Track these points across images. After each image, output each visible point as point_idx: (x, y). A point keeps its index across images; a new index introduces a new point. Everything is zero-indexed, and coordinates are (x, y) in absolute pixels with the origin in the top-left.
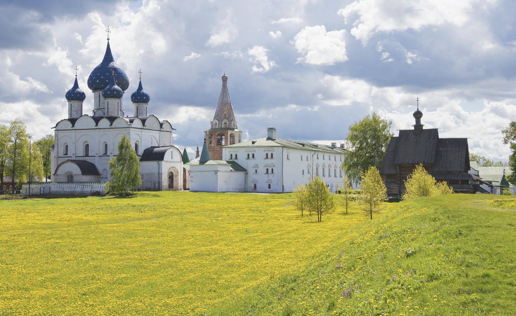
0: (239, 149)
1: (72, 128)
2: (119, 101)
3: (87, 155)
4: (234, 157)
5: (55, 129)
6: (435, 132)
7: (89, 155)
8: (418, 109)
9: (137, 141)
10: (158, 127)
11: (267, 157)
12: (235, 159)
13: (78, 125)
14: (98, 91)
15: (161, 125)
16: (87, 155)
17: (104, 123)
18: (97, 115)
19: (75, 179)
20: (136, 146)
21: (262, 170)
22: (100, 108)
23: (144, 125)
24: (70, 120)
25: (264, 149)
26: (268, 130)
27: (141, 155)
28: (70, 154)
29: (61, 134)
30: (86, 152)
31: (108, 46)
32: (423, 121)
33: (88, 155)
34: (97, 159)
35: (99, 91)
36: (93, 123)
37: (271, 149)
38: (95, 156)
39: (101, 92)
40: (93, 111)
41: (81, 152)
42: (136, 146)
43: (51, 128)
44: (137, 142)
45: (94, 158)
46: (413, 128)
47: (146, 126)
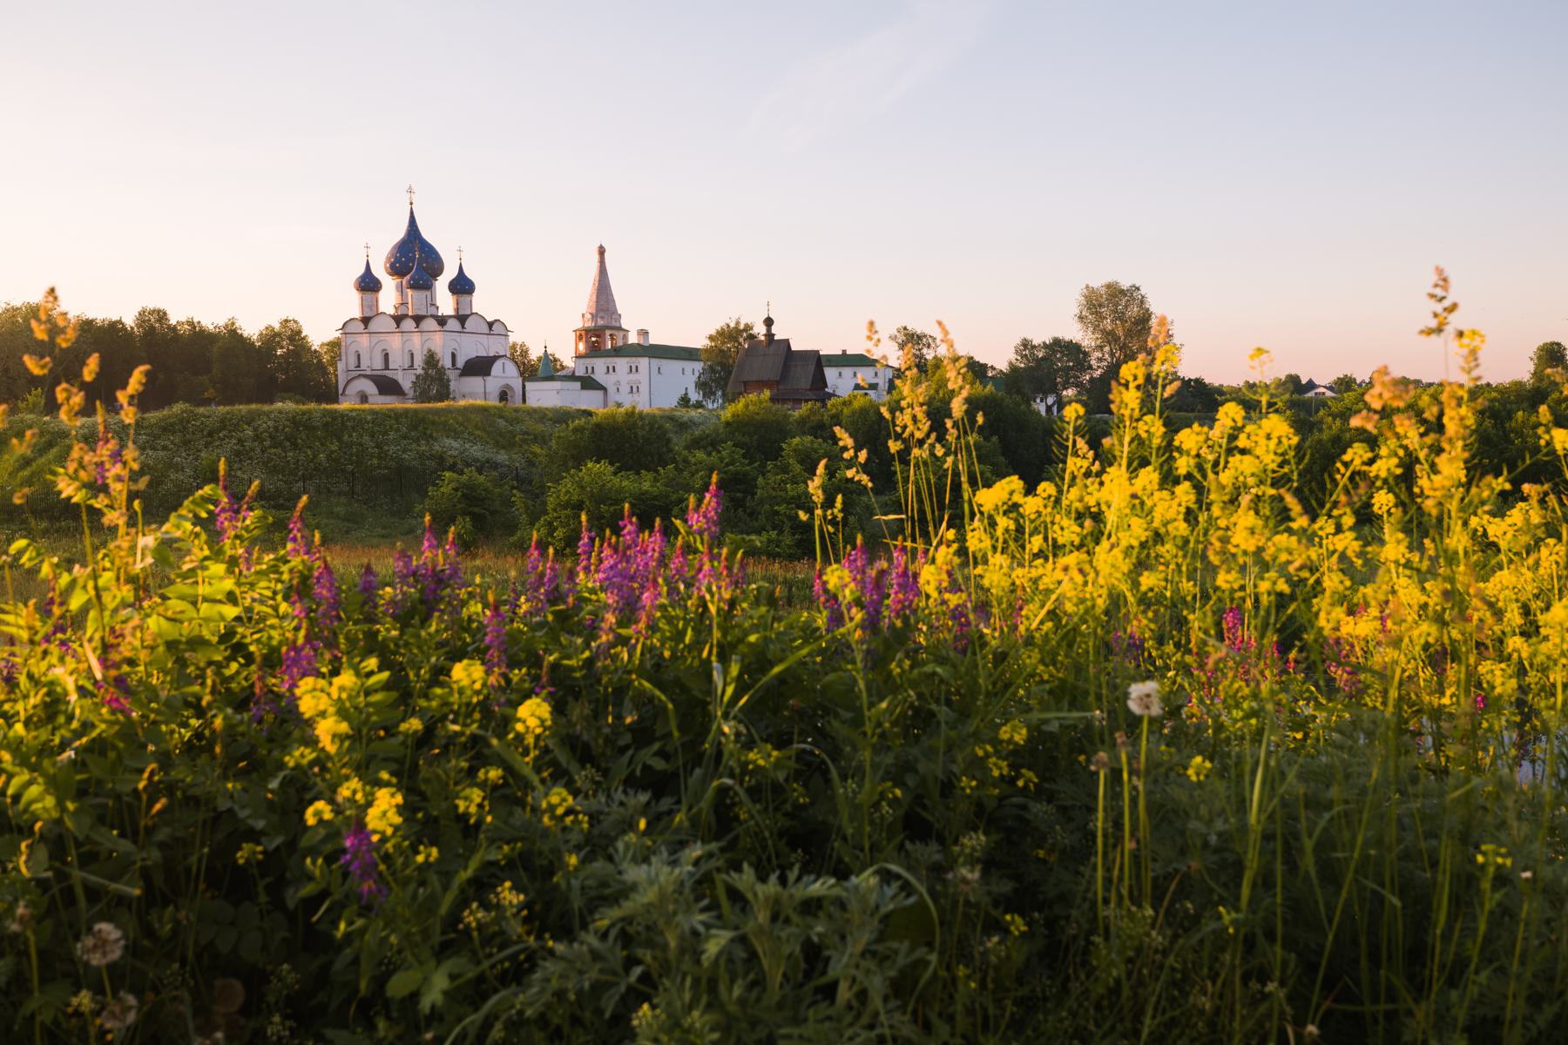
2: (428, 293)
6: (787, 342)
13: (373, 326)
16: (387, 368)
17: (409, 324)
19: (370, 399)
21: (625, 389)
28: (363, 366)
29: (350, 339)
31: (412, 213)
32: (774, 330)
34: (400, 373)
41: (378, 363)
42: (453, 355)
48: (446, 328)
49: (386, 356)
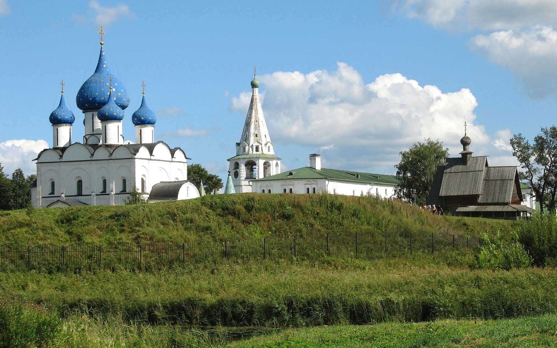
0: (272, 182)
1: (59, 160)
3: (80, 194)
5: (36, 161)
7: (83, 194)
8: (465, 135)
9: (144, 175)
13: (67, 156)
14: (90, 112)
15: (173, 152)
16: (80, 194)
18: (90, 142)
20: (143, 182)
24: (55, 149)
25: (304, 182)
26: (311, 158)
27: (149, 193)
29: (44, 167)
30: (78, 190)
32: (470, 149)
33: (82, 193)
36: (85, 154)
37: (312, 181)
38: (91, 195)
39: (96, 113)
40: (84, 137)
42: (143, 182)
44: (143, 177)
45: (89, 197)
46: (460, 156)
49: (80, 183)
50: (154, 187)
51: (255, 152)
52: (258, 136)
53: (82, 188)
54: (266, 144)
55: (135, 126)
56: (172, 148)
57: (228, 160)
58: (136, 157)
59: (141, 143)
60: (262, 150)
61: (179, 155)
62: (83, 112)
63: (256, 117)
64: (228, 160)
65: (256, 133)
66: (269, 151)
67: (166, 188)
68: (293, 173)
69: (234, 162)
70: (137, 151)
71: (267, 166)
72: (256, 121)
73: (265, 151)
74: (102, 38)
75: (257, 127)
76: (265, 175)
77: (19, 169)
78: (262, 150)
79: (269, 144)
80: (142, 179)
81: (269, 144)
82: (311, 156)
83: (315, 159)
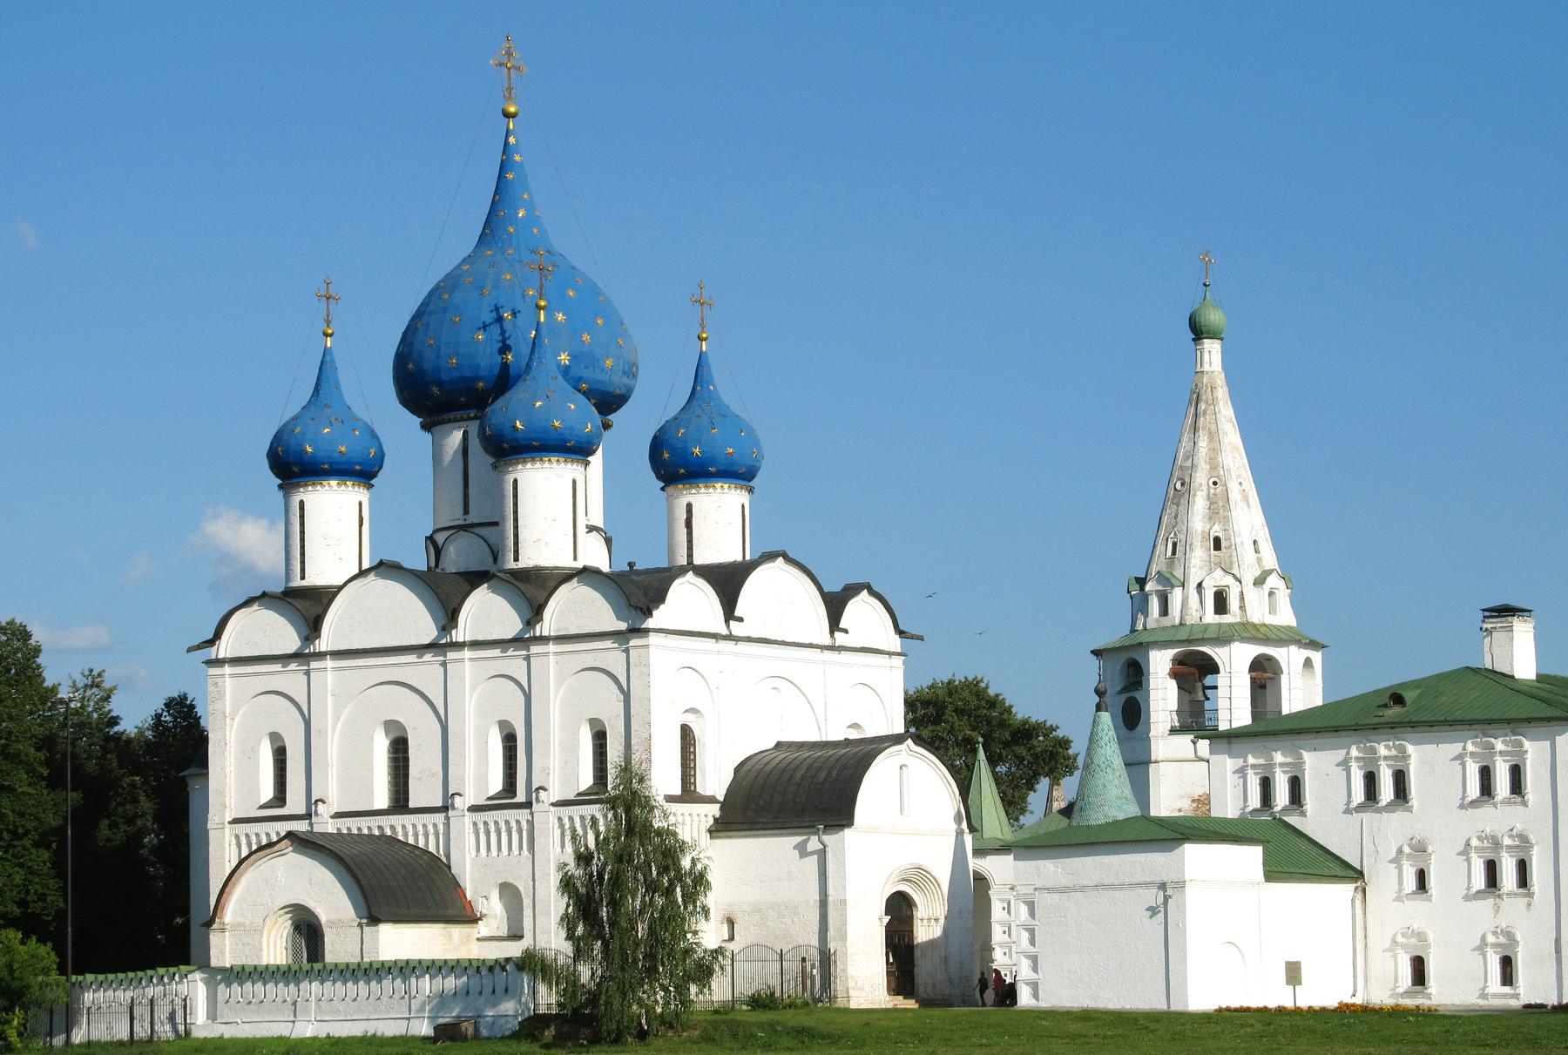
3: (400, 802)
4: (1282, 796)
7: (411, 805)
10: (817, 628)
11: (1487, 788)
12: (1284, 810)
14: (450, 421)
15: (835, 605)
22: (472, 519)
23: (729, 613)
27: (721, 799)
33: (407, 800)
35: (462, 419)
40: (430, 539)
43: (190, 650)
44: (690, 719)
47: (741, 620)
48: (660, 617)
50: (745, 768)
51: (1210, 617)
52: (1223, 544)
53: (406, 776)
54: (1259, 582)
55: (663, 489)
56: (834, 586)
57: (1096, 653)
58: (650, 623)
59: (690, 556)
60: (1242, 608)
61: (864, 616)
62: (426, 427)
63: (1214, 466)
64: (1096, 653)
65: (1217, 530)
66: (1272, 610)
67: (799, 774)
68: (1409, 696)
69: (1124, 657)
70: (660, 597)
71: (1264, 675)
72: (1215, 483)
73: (1258, 613)
74: (510, 89)
75: (1219, 507)
76: (1255, 715)
77: (184, 697)
78: (1242, 608)
79: (1274, 581)
80: (686, 732)
81: (1274, 581)
82: (1487, 614)
83: (1510, 629)
